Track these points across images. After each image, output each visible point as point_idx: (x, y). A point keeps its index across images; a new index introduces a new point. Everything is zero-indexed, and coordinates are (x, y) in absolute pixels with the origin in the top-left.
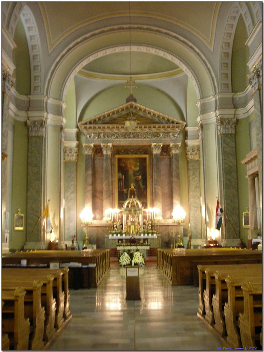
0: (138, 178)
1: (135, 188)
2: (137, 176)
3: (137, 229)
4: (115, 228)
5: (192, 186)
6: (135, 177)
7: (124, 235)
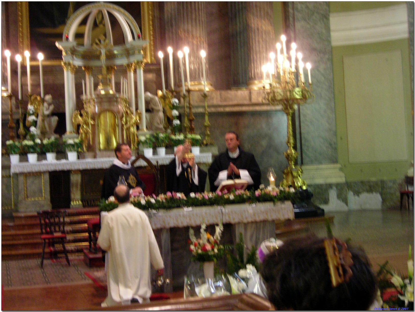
3: (128, 129)
4: (33, 129)
7: (72, 156)
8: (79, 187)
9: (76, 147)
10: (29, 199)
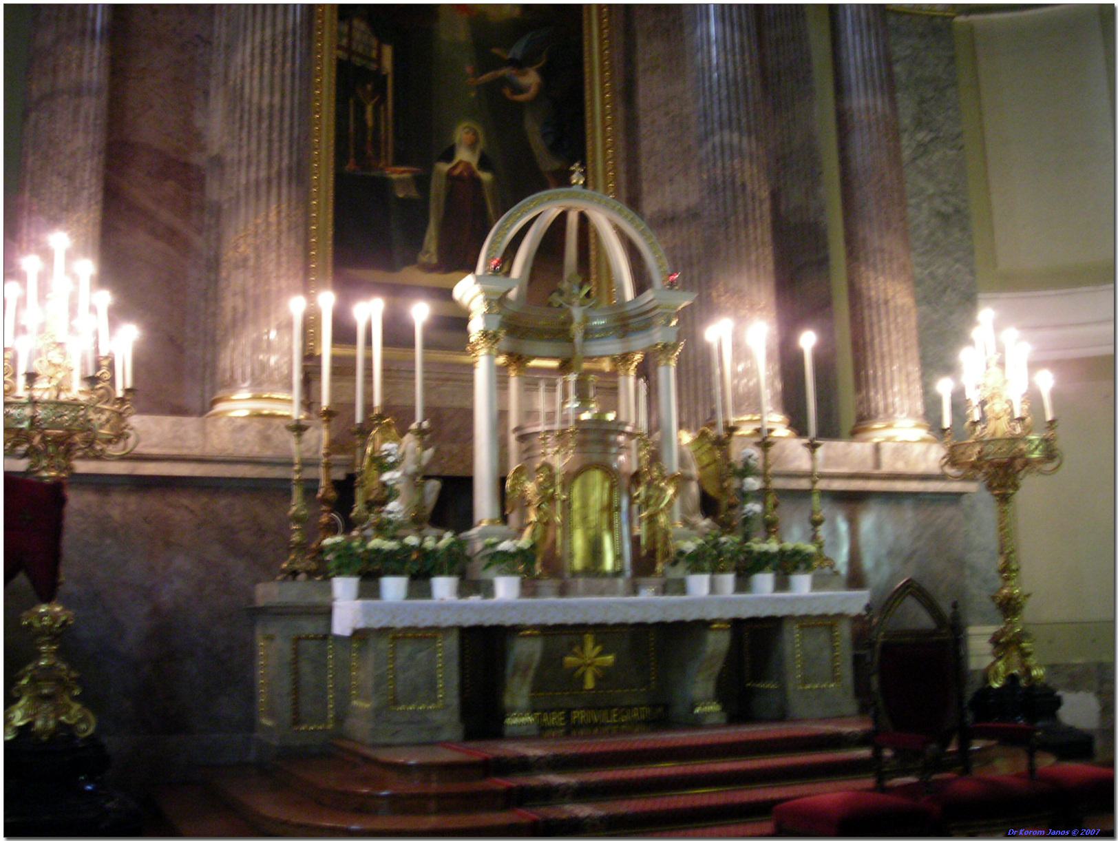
0: (519, 90)
1: (484, 163)
2: (506, 72)
5: (918, 206)
6: (487, 77)
8: (531, 673)
9: (519, 562)
10: (401, 708)
